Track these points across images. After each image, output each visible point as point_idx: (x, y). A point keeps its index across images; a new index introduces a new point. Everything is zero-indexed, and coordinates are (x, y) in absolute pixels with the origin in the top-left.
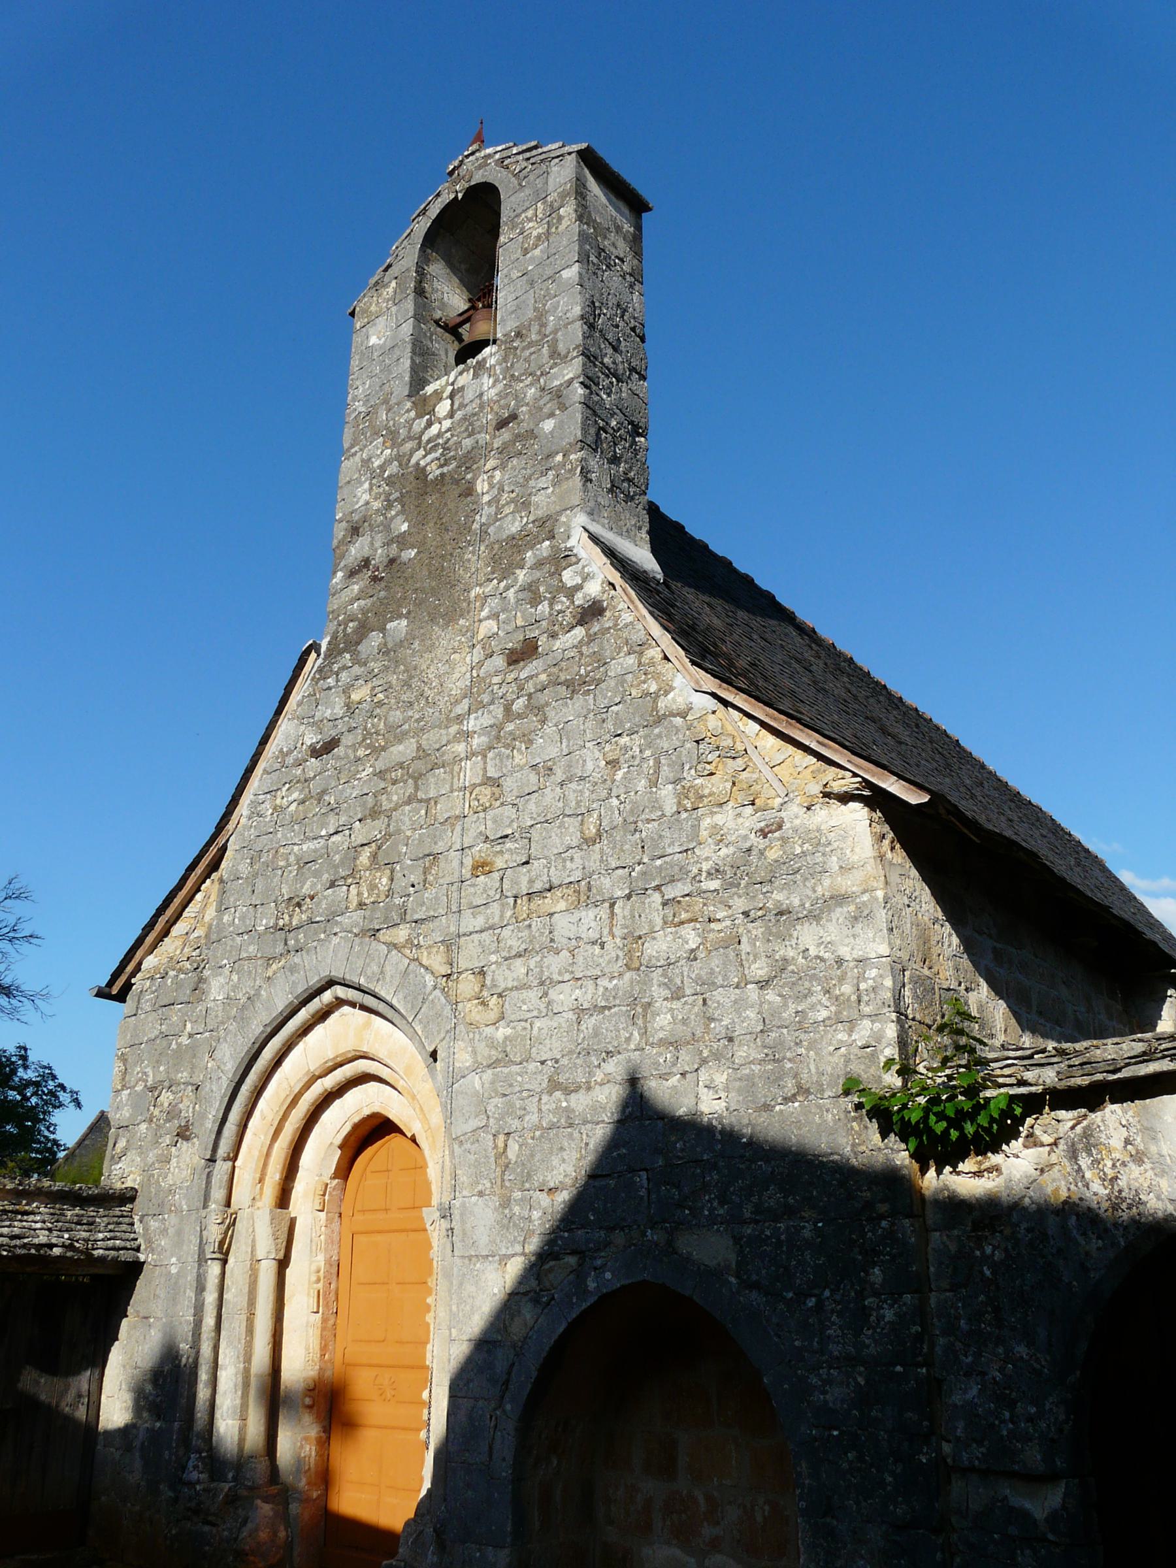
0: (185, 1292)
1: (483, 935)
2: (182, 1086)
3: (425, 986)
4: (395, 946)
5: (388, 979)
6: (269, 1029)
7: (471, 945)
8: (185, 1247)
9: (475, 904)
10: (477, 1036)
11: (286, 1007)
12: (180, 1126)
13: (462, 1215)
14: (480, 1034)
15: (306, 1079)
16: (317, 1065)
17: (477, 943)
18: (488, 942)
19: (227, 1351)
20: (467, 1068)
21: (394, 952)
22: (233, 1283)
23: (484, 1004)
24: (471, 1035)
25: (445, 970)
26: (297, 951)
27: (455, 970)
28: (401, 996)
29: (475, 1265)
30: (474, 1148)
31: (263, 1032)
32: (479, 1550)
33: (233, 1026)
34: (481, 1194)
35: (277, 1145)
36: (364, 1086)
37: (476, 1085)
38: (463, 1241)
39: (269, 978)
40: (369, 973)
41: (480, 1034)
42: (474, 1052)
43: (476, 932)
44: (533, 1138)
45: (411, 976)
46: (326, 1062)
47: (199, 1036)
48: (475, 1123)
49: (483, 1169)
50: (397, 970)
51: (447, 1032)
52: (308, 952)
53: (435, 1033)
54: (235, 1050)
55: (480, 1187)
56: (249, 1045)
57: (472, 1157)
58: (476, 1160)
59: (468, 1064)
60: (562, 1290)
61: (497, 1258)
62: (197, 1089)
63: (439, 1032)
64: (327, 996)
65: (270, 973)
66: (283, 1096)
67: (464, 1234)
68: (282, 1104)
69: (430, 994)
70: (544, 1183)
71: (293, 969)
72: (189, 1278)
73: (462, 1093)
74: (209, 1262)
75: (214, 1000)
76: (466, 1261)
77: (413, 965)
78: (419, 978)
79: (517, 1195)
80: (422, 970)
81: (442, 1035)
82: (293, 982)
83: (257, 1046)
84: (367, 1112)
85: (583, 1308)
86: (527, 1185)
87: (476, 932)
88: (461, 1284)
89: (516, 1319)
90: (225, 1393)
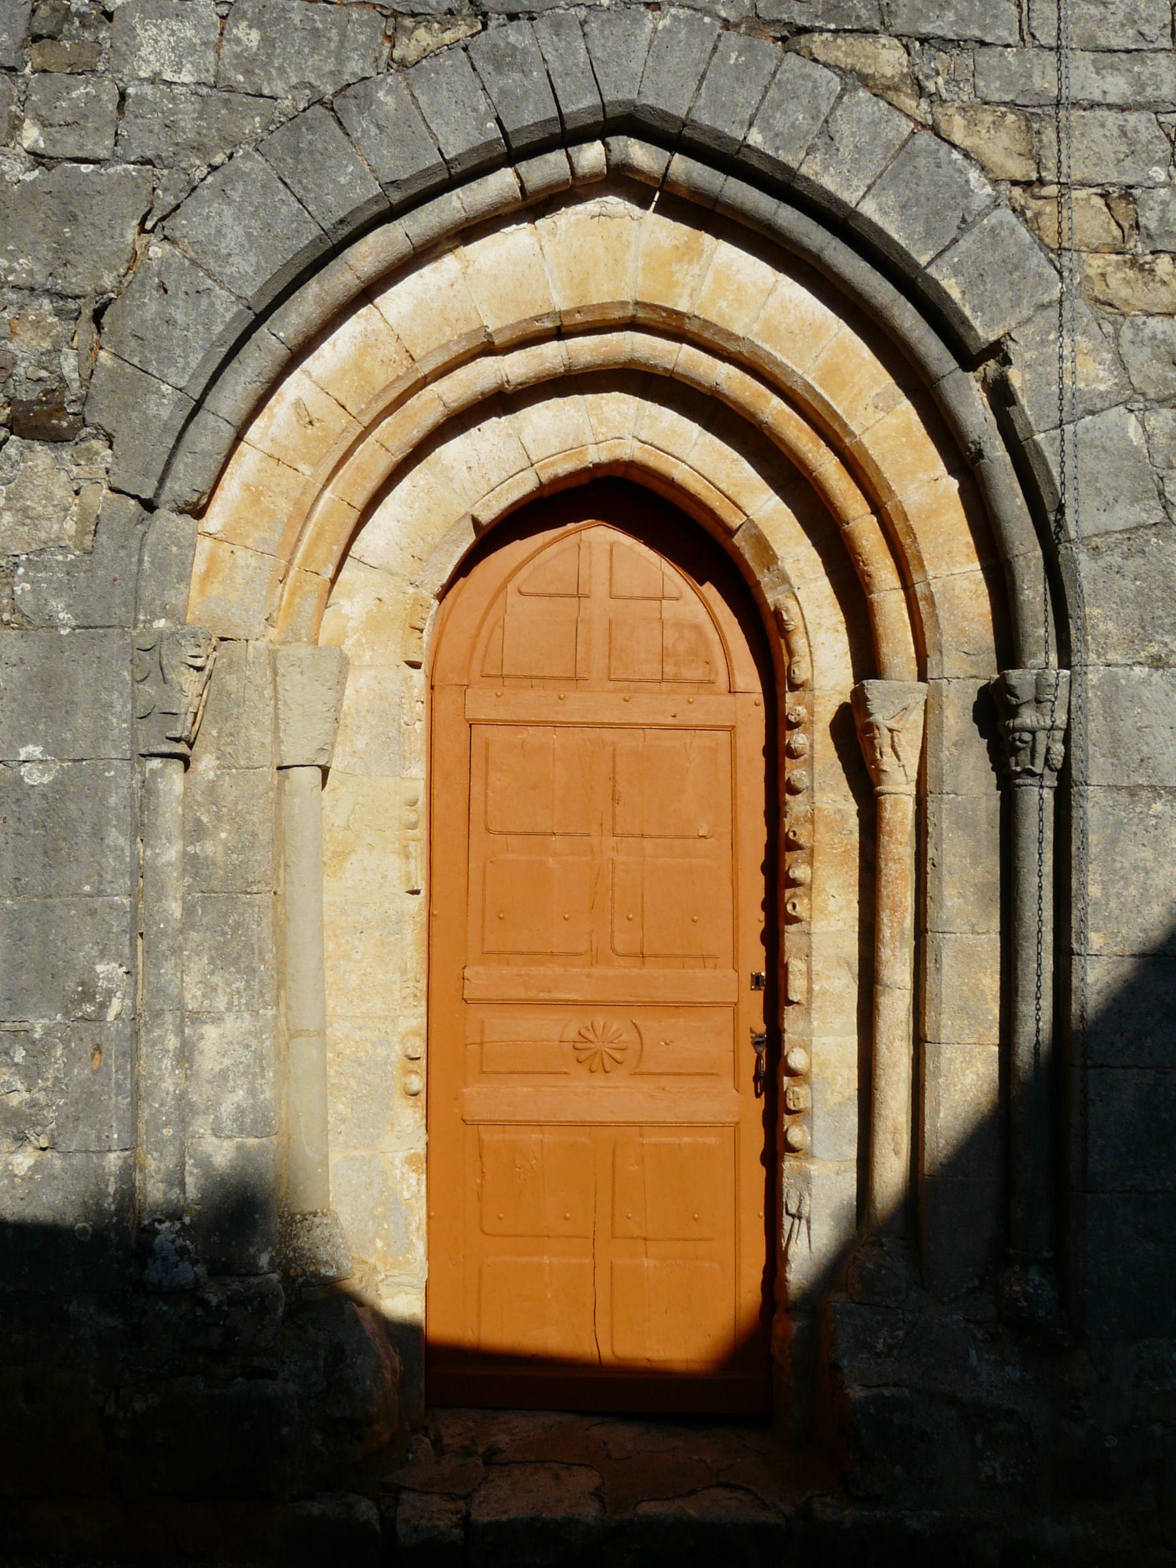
0: (98, 835)
1: (1133, 118)
2: (12, 296)
3: (967, 193)
4: (865, 80)
5: (845, 152)
6: (396, 197)
7: (1096, 133)
8: (80, 721)
9: (1103, 42)
10: (1127, 333)
11: (474, 150)
12: (10, 402)
13: (1108, 701)
14: (1137, 329)
15: (458, 349)
16: (511, 319)
17: (1116, 132)
18: (1144, 136)
19: (216, 979)
20: (1101, 395)
21: (863, 94)
22: (219, 818)
23: (1134, 263)
24: (1108, 328)
25: (1020, 169)
26: (513, 17)
27: (1048, 176)
28: (890, 200)
29: (1149, 806)
30: (1132, 565)
31: (376, 200)
33: (253, 166)
35: (327, 494)
36: (590, 397)
37: (1131, 434)
38: (1115, 755)
39: (403, 64)
40: (780, 123)
41: (1137, 329)
42: (1121, 362)
43: (1110, 106)
45: (922, 162)
46: (538, 319)
47: (85, 168)
48: (1127, 515)
49: (1160, 613)
50: (875, 136)
51: (1043, 307)
52: (557, 26)
53: (1005, 305)
54: (268, 227)
55: (1154, 649)
56: (327, 225)
57: (1129, 587)
58: (1140, 592)
59: (1102, 388)
62: (98, 316)
63: (1016, 303)
64: (591, 156)
65: (407, 49)
66: (382, 377)
67: (1115, 738)
68: (377, 397)
69: (984, 213)
71: (503, 59)
72: (113, 800)
73: (1092, 445)
74: (156, 763)
75: (155, 80)
76: (1124, 797)
77: (925, 139)
78: (946, 170)
80: (956, 155)
81: (1026, 312)
82: (503, 92)
83: (345, 231)
84: (596, 455)
87: (1110, 106)
88: (1114, 841)
90: (223, 1075)
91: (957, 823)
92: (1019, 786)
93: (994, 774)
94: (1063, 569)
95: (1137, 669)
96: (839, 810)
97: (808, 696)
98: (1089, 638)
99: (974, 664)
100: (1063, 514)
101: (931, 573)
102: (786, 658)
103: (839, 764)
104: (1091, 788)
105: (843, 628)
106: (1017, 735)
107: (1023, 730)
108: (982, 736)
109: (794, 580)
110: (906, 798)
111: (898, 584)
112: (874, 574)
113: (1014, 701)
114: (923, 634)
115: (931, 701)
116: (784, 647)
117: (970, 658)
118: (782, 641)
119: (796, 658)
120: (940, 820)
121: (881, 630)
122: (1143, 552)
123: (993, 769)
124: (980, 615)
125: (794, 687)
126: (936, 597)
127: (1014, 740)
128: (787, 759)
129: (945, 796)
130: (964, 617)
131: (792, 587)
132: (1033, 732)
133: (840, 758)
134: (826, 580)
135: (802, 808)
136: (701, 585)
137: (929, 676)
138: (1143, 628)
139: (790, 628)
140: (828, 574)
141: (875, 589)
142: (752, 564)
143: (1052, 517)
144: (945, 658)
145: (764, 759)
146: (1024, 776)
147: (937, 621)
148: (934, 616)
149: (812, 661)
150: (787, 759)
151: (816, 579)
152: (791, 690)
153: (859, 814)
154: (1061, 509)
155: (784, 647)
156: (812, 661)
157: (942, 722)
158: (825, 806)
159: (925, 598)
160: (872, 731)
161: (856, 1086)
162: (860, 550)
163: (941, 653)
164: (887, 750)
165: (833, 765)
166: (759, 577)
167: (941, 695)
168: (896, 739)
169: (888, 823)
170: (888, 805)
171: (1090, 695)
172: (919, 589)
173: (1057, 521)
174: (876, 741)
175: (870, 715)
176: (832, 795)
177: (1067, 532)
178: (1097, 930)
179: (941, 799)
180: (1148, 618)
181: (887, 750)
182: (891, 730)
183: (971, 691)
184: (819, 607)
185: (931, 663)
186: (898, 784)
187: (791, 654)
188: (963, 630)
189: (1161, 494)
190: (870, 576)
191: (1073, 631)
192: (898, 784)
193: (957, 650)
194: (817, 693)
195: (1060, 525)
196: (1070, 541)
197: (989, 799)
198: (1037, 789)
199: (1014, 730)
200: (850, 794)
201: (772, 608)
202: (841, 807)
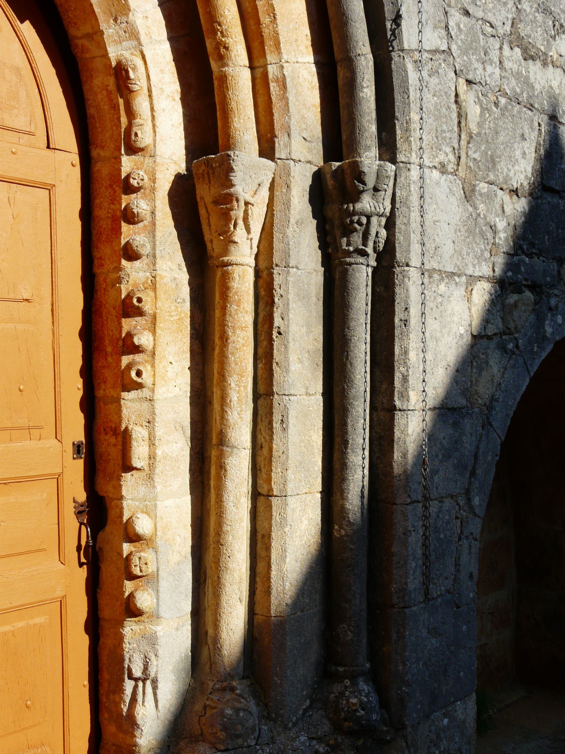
32: (445, 715)
34: (443, 169)
44: (496, 104)
49: (445, 127)
55: (441, 157)
60: (525, 335)
61: (464, 279)
70: (507, 179)
79: (483, 187)
85: (542, 358)
86: (492, 177)
89: (484, 373)
91: (298, 295)
92: (350, 264)
93: (320, 252)
94: (394, 74)
95: (434, 171)
96: (175, 279)
97: (148, 161)
98: (412, 139)
99: (310, 150)
100: (398, 25)
101: (285, 57)
102: (124, 120)
103: (175, 233)
104: (411, 269)
105: (178, 96)
106: (356, 218)
107: (362, 214)
108: (314, 217)
109: (143, 38)
110: (248, 268)
111: (247, 63)
112: (231, 47)
113: (361, 187)
114: (272, 115)
115: (277, 179)
116: (122, 108)
117: (308, 144)
118: (121, 101)
119: (138, 121)
120: (287, 292)
121: (233, 105)
122: (438, 72)
123: (320, 248)
124: (314, 106)
125: (133, 150)
126: (288, 80)
127: (352, 222)
128: (123, 224)
129: (291, 270)
130: (304, 105)
131: (140, 44)
132: (369, 217)
133: (176, 227)
134: (167, 46)
135: (141, 274)
136: (22, 22)
137: (277, 155)
138: (437, 137)
139: (135, 88)
140: (170, 39)
141: (230, 63)
142: (97, 10)
143: (388, 25)
144: (293, 141)
145: (80, 223)
146: (355, 255)
147: (287, 104)
148: (284, 98)
149: (154, 126)
150: (123, 224)
151: (159, 42)
152: (128, 154)
153: (190, 283)
154: (397, 18)
155: (122, 108)
156: (154, 126)
157: (289, 200)
158: (165, 274)
159: (277, 81)
160: (231, 201)
161: (191, 544)
162: (221, 19)
163: (289, 135)
164: (241, 223)
165: (170, 233)
166: (103, 26)
167: (289, 175)
168: (250, 212)
169: (236, 293)
170: (236, 275)
171: (412, 189)
172: (272, 70)
173: (393, 31)
174: (232, 213)
175: (232, 185)
176: (169, 264)
177: (401, 42)
178: (413, 390)
179: (288, 272)
180: (439, 130)
181: (241, 223)
182: (247, 204)
183: (308, 174)
184: (162, 71)
185: (280, 143)
186: (244, 256)
187: (131, 114)
188: (303, 117)
189: (447, 27)
190: (227, 48)
191: (398, 132)
192: (244, 256)
193: (300, 134)
194: (158, 160)
195: (396, 32)
196: (402, 50)
197: (317, 275)
198: (364, 267)
199: (354, 213)
200: (183, 264)
201: (114, 64)
202: (176, 276)
